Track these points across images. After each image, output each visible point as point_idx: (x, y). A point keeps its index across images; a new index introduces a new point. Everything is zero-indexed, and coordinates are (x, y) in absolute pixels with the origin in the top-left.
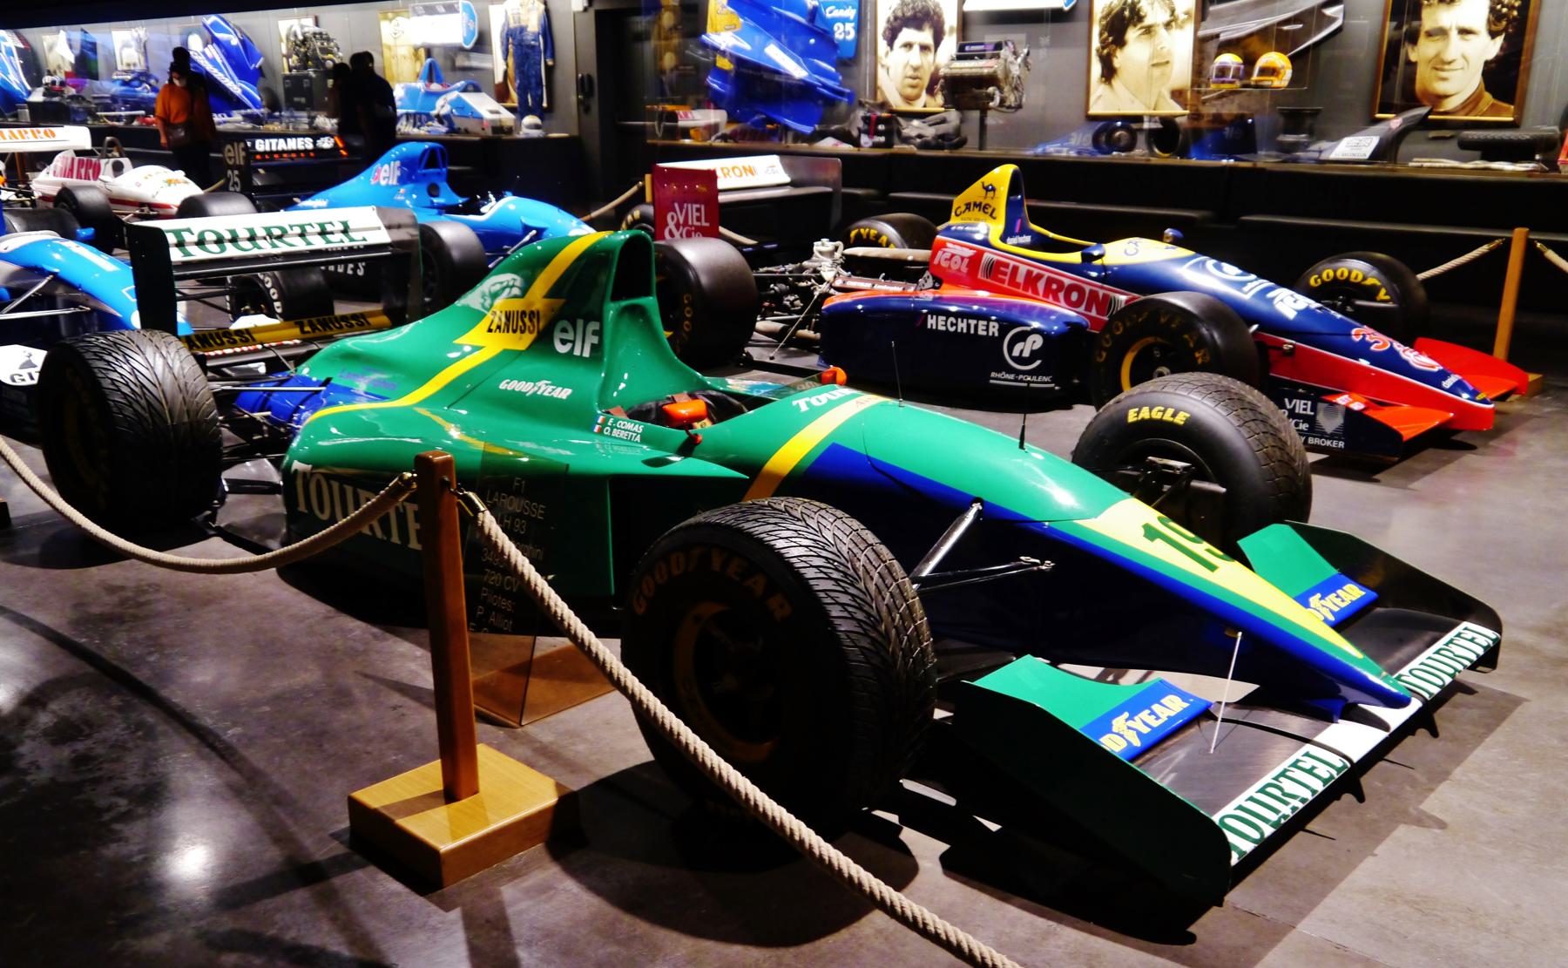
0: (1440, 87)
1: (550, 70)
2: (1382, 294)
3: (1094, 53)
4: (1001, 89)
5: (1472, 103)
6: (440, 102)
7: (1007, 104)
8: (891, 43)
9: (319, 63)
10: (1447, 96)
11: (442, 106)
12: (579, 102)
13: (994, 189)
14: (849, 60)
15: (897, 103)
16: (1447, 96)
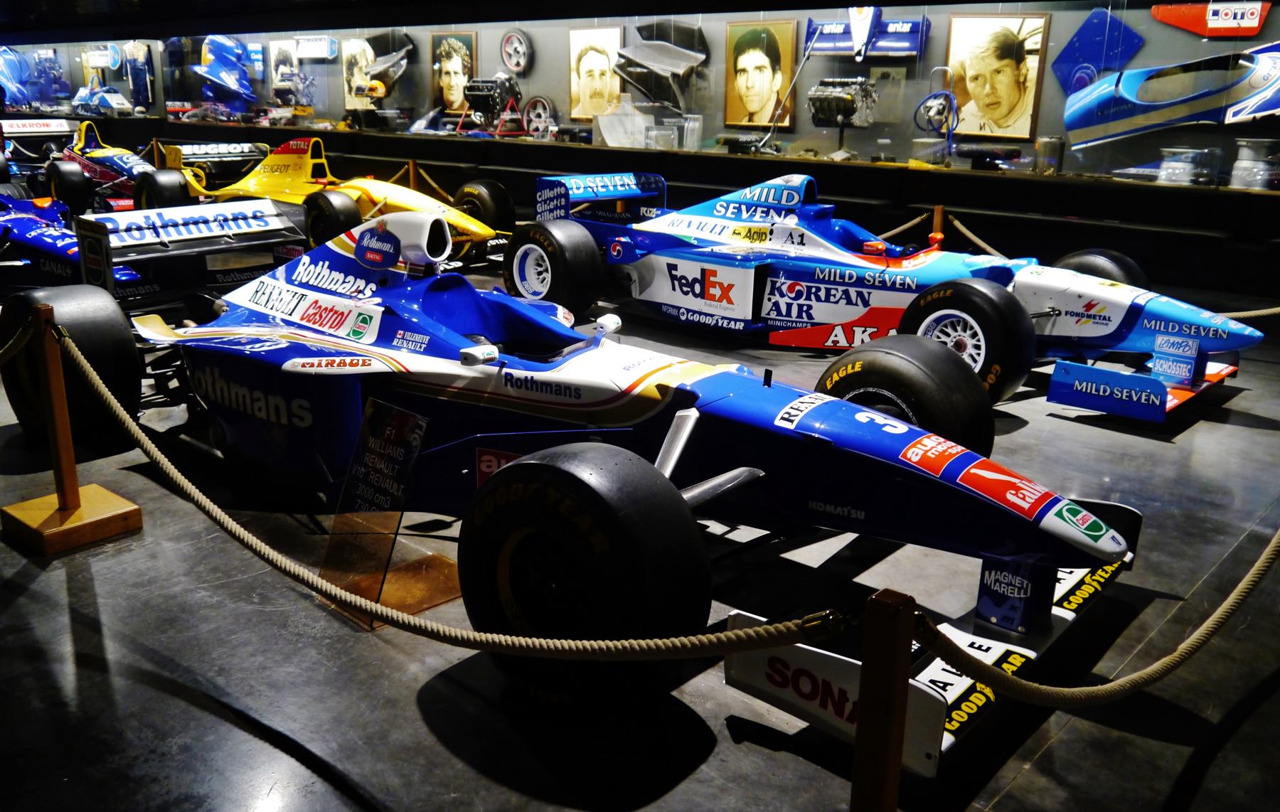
0: (452, 98)
1: (152, 82)
4: (295, 96)
5: (462, 106)
9: (47, 75)
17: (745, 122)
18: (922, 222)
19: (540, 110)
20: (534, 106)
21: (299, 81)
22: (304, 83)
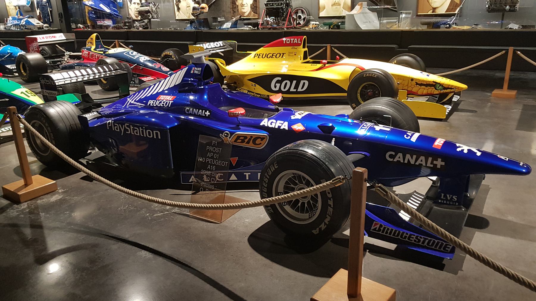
0: (243, 11)
2: (173, 57)
3: (175, 4)
4: (152, 14)
5: (250, 13)
6: (22, 21)
7: (154, 17)
8: (131, 3)
10: (245, 13)
11: (23, 22)
12: (60, 20)
13: (92, 39)
14: (122, 7)
15: (135, 18)
16: (245, 13)
17: (430, 13)
18: (324, 50)
19: (300, 14)
20: (296, 13)
21: (152, 6)
22: (155, 7)
